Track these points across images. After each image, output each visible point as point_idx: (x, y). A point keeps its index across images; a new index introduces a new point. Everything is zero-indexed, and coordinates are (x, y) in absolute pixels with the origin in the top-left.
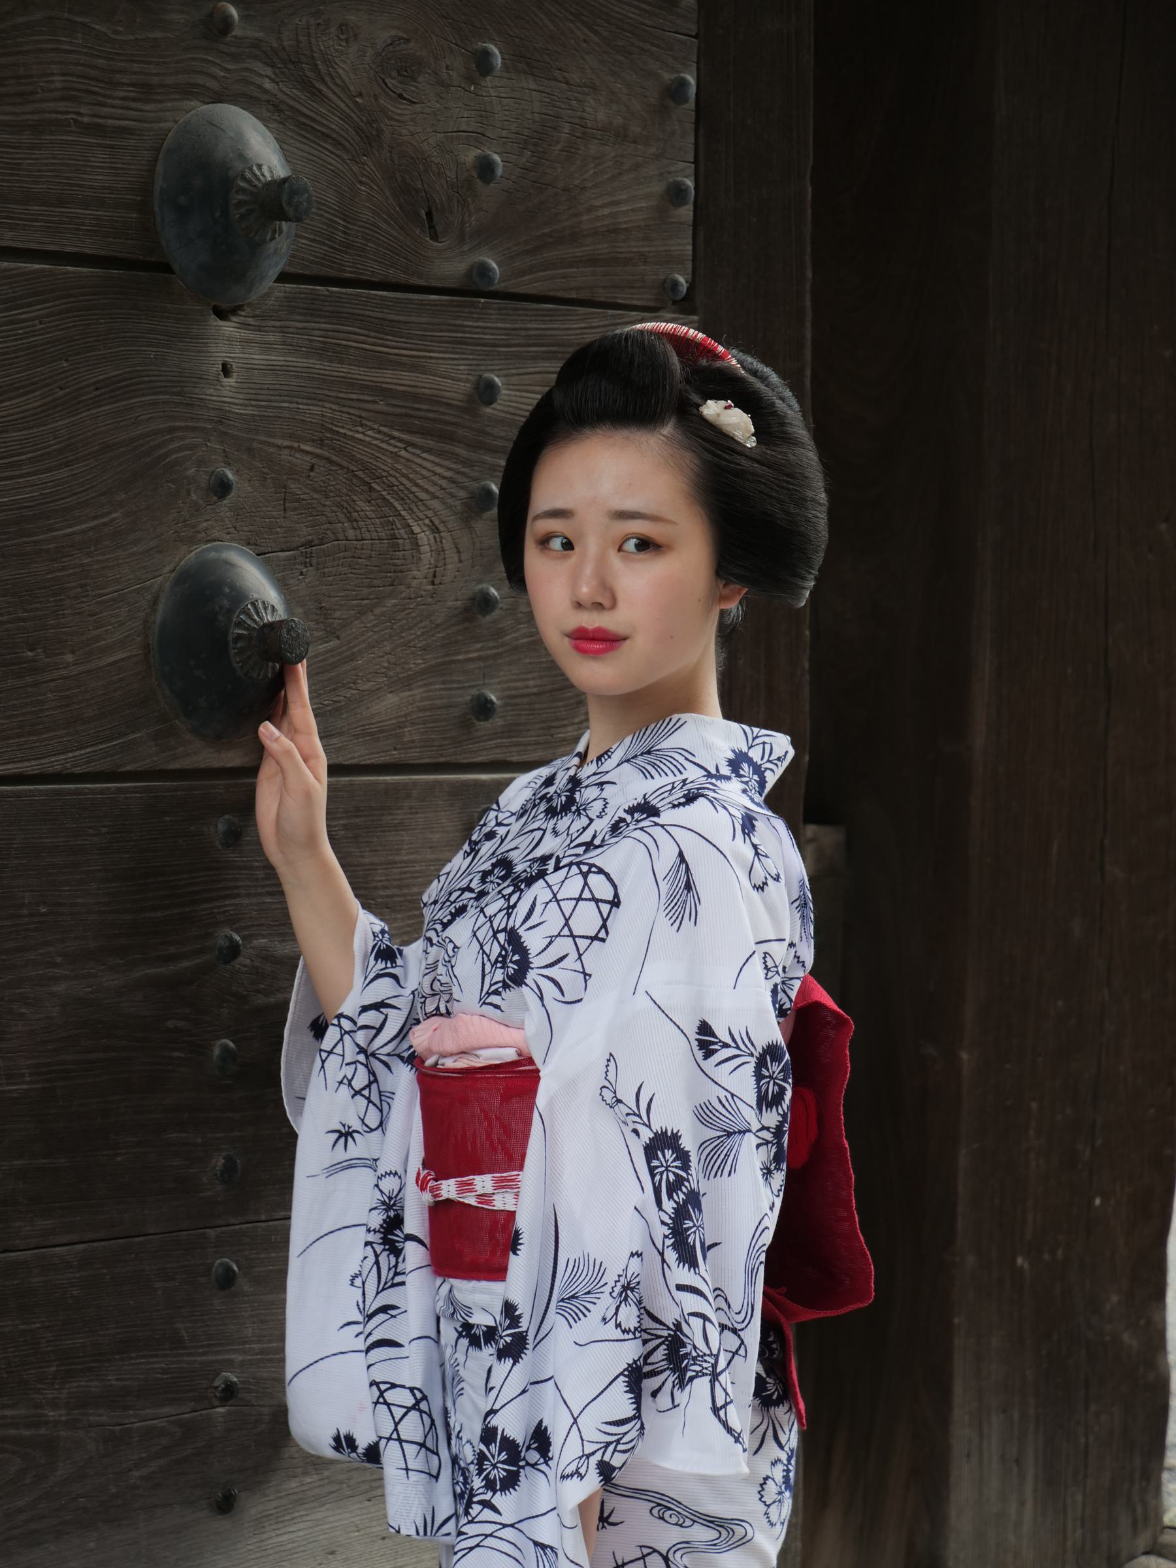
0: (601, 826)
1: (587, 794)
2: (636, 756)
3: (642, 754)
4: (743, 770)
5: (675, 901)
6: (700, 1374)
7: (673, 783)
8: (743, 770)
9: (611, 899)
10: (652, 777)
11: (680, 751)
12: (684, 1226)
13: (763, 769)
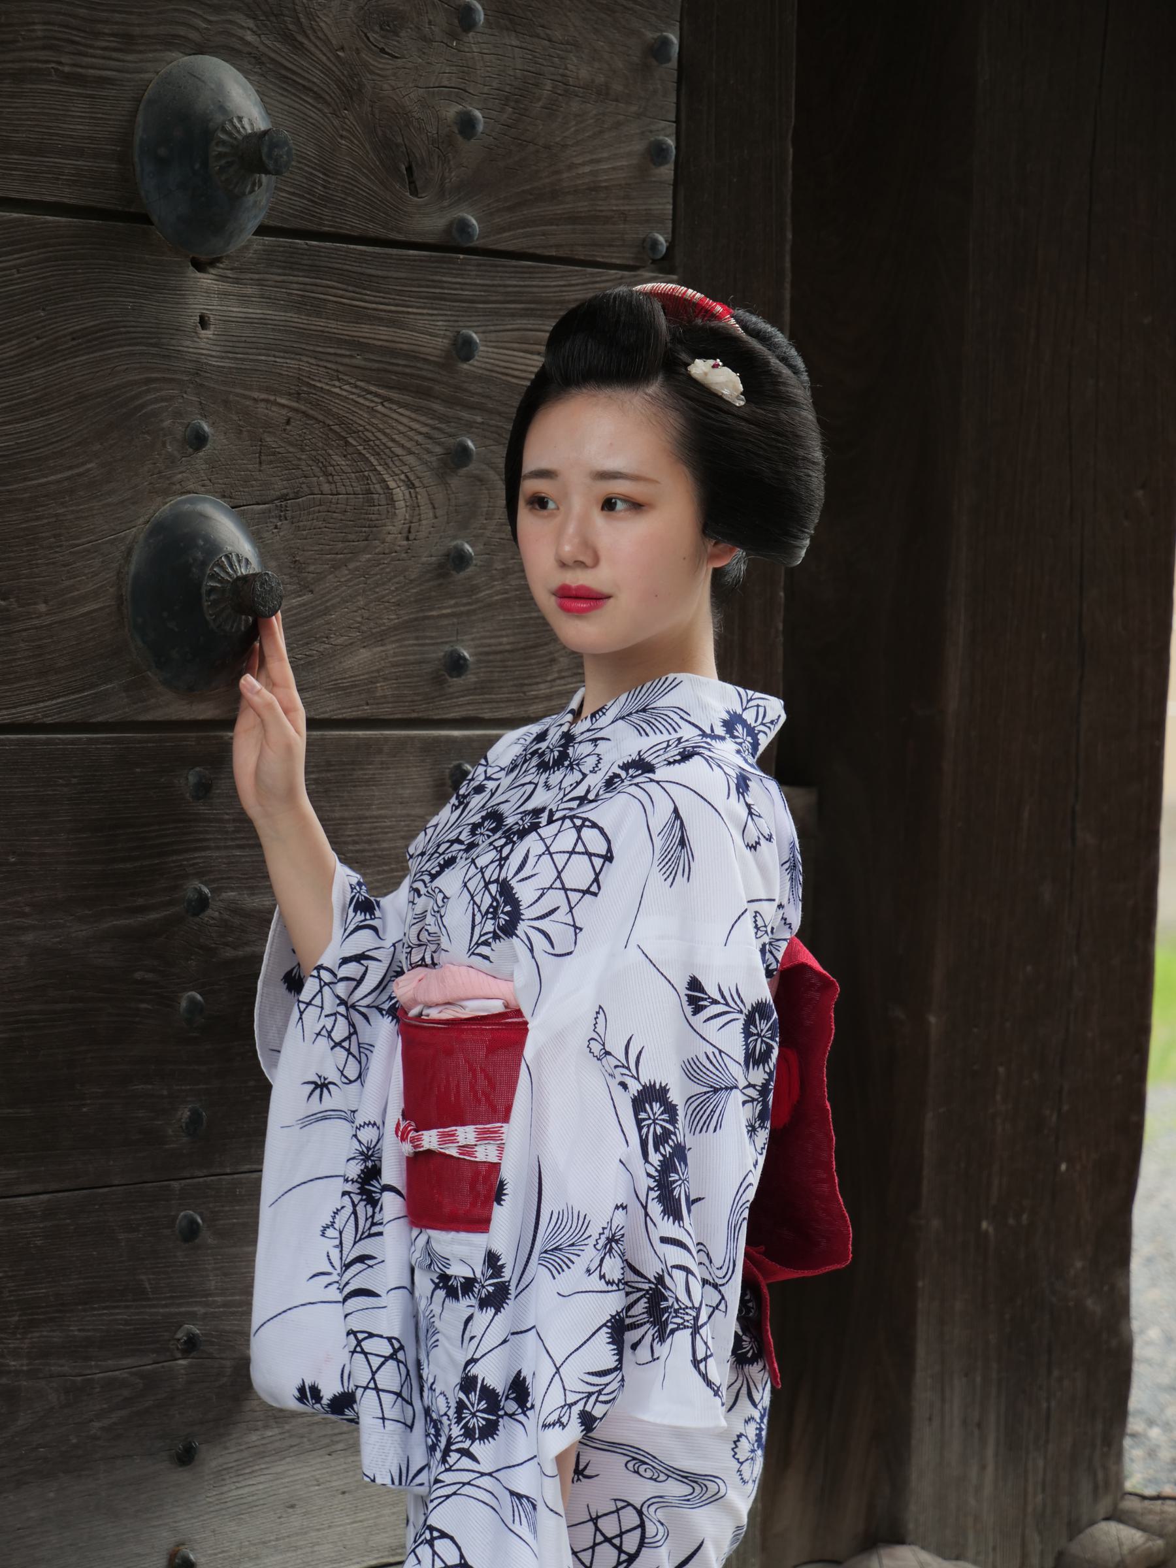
0: (595, 781)
1: (580, 750)
2: (631, 713)
5: (669, 856)
7: (668, 741)
9: (604, 853)
10: (647, 735)
11: (675, 710)
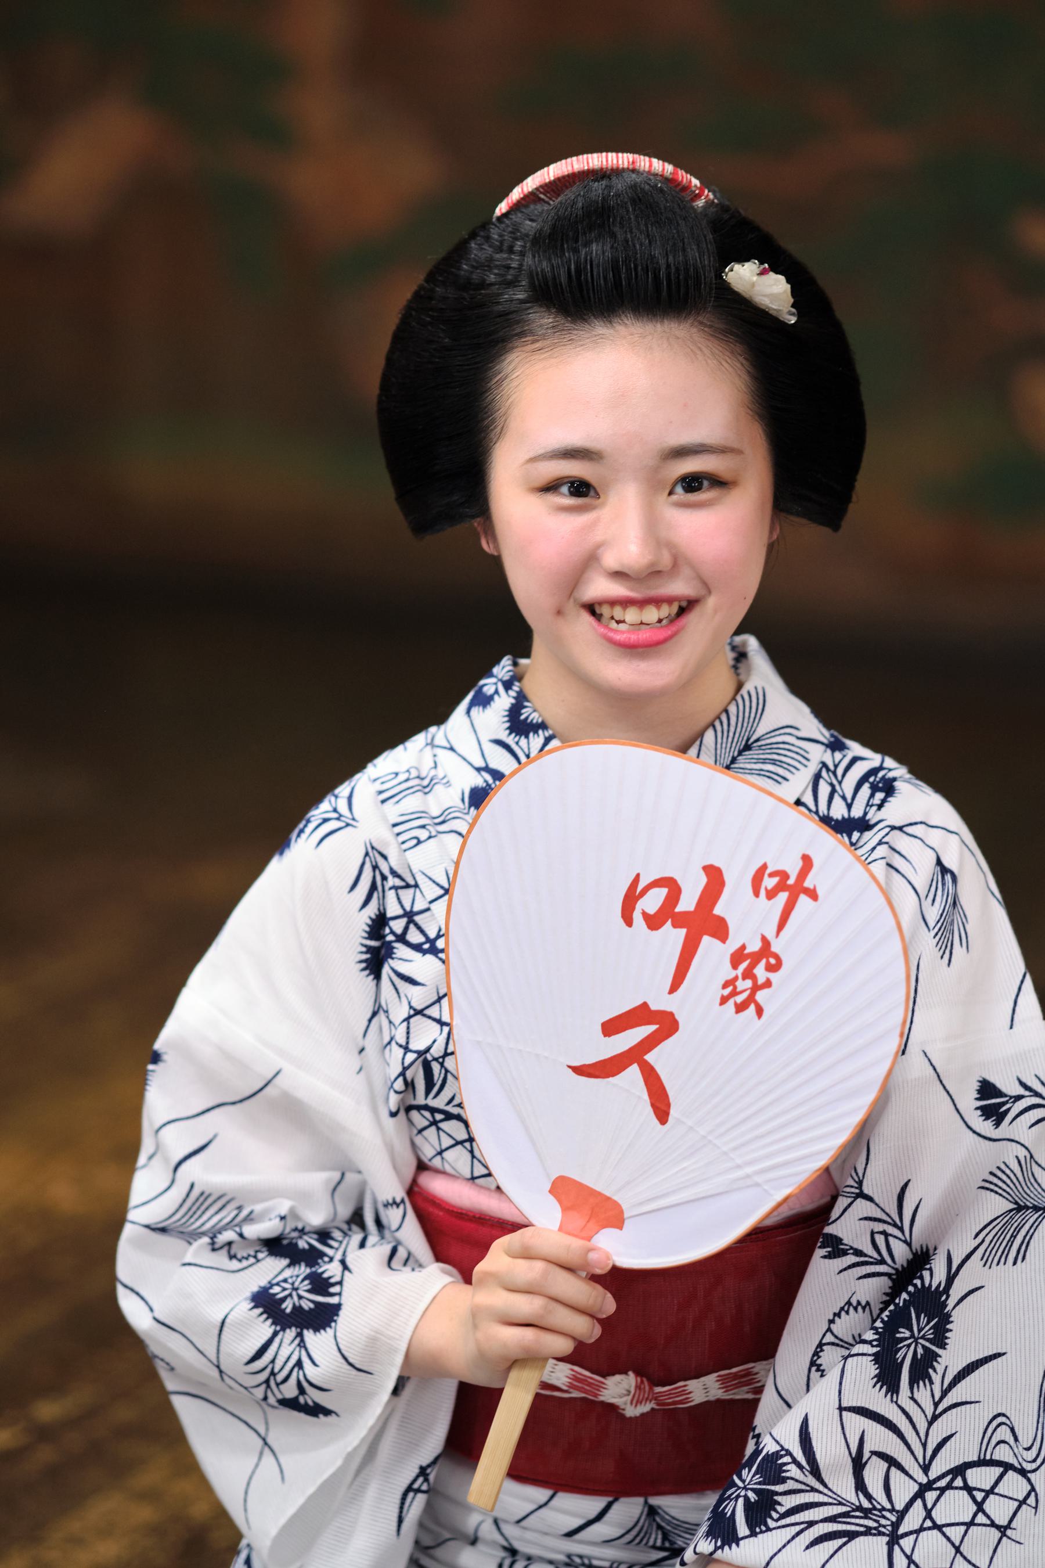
6: (874, 1531)
12: (898, 1335)
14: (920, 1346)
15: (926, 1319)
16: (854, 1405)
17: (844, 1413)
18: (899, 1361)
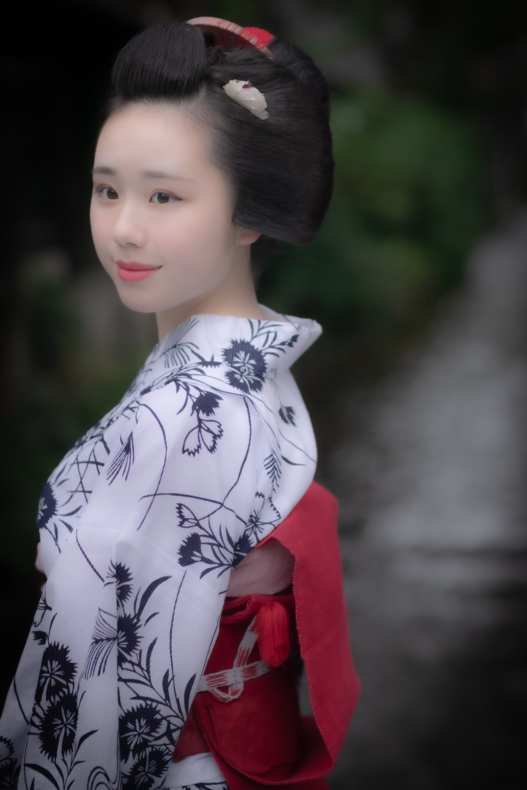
2: (168, 350)
3: (171, 349)
4: (238, 357)
8: (238, 357)
12: (54, 723)
13: (262, 354)
14: (68, 729)
15: (70, 713)
16: (31, 763)
17: (26, 767)
18: (56, 737)
